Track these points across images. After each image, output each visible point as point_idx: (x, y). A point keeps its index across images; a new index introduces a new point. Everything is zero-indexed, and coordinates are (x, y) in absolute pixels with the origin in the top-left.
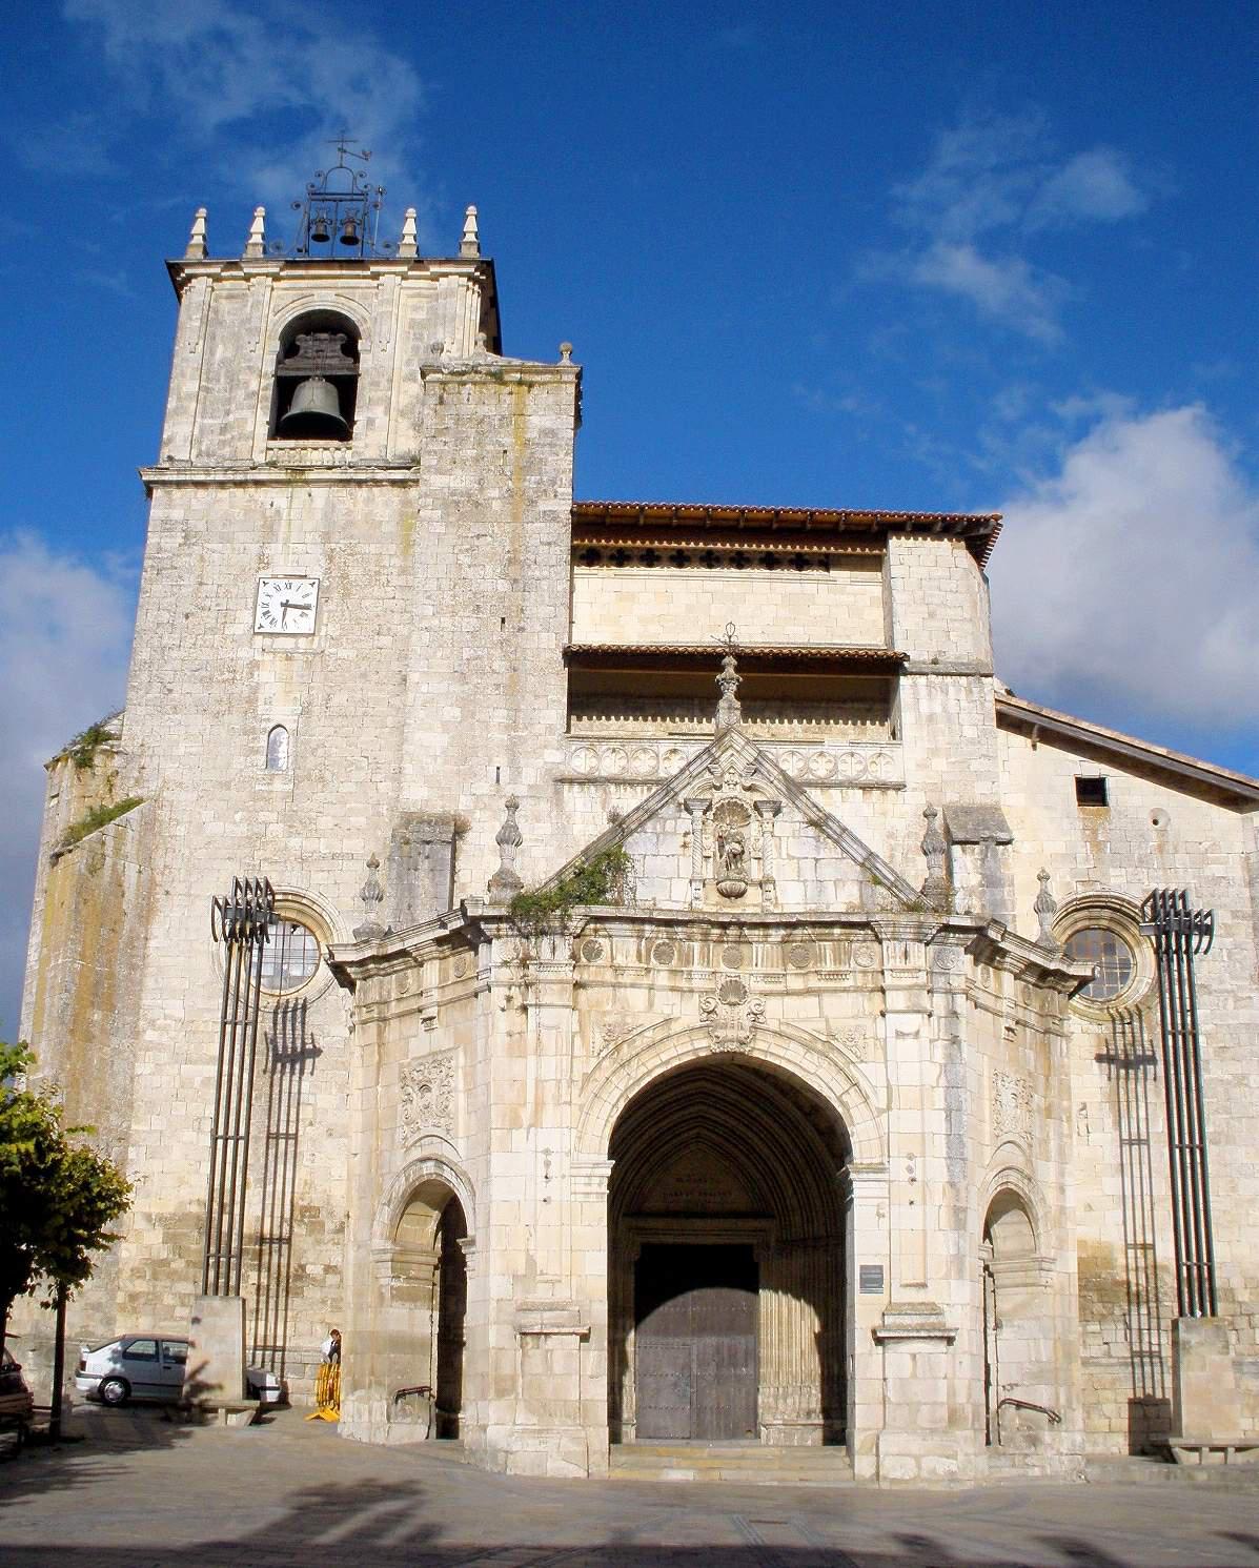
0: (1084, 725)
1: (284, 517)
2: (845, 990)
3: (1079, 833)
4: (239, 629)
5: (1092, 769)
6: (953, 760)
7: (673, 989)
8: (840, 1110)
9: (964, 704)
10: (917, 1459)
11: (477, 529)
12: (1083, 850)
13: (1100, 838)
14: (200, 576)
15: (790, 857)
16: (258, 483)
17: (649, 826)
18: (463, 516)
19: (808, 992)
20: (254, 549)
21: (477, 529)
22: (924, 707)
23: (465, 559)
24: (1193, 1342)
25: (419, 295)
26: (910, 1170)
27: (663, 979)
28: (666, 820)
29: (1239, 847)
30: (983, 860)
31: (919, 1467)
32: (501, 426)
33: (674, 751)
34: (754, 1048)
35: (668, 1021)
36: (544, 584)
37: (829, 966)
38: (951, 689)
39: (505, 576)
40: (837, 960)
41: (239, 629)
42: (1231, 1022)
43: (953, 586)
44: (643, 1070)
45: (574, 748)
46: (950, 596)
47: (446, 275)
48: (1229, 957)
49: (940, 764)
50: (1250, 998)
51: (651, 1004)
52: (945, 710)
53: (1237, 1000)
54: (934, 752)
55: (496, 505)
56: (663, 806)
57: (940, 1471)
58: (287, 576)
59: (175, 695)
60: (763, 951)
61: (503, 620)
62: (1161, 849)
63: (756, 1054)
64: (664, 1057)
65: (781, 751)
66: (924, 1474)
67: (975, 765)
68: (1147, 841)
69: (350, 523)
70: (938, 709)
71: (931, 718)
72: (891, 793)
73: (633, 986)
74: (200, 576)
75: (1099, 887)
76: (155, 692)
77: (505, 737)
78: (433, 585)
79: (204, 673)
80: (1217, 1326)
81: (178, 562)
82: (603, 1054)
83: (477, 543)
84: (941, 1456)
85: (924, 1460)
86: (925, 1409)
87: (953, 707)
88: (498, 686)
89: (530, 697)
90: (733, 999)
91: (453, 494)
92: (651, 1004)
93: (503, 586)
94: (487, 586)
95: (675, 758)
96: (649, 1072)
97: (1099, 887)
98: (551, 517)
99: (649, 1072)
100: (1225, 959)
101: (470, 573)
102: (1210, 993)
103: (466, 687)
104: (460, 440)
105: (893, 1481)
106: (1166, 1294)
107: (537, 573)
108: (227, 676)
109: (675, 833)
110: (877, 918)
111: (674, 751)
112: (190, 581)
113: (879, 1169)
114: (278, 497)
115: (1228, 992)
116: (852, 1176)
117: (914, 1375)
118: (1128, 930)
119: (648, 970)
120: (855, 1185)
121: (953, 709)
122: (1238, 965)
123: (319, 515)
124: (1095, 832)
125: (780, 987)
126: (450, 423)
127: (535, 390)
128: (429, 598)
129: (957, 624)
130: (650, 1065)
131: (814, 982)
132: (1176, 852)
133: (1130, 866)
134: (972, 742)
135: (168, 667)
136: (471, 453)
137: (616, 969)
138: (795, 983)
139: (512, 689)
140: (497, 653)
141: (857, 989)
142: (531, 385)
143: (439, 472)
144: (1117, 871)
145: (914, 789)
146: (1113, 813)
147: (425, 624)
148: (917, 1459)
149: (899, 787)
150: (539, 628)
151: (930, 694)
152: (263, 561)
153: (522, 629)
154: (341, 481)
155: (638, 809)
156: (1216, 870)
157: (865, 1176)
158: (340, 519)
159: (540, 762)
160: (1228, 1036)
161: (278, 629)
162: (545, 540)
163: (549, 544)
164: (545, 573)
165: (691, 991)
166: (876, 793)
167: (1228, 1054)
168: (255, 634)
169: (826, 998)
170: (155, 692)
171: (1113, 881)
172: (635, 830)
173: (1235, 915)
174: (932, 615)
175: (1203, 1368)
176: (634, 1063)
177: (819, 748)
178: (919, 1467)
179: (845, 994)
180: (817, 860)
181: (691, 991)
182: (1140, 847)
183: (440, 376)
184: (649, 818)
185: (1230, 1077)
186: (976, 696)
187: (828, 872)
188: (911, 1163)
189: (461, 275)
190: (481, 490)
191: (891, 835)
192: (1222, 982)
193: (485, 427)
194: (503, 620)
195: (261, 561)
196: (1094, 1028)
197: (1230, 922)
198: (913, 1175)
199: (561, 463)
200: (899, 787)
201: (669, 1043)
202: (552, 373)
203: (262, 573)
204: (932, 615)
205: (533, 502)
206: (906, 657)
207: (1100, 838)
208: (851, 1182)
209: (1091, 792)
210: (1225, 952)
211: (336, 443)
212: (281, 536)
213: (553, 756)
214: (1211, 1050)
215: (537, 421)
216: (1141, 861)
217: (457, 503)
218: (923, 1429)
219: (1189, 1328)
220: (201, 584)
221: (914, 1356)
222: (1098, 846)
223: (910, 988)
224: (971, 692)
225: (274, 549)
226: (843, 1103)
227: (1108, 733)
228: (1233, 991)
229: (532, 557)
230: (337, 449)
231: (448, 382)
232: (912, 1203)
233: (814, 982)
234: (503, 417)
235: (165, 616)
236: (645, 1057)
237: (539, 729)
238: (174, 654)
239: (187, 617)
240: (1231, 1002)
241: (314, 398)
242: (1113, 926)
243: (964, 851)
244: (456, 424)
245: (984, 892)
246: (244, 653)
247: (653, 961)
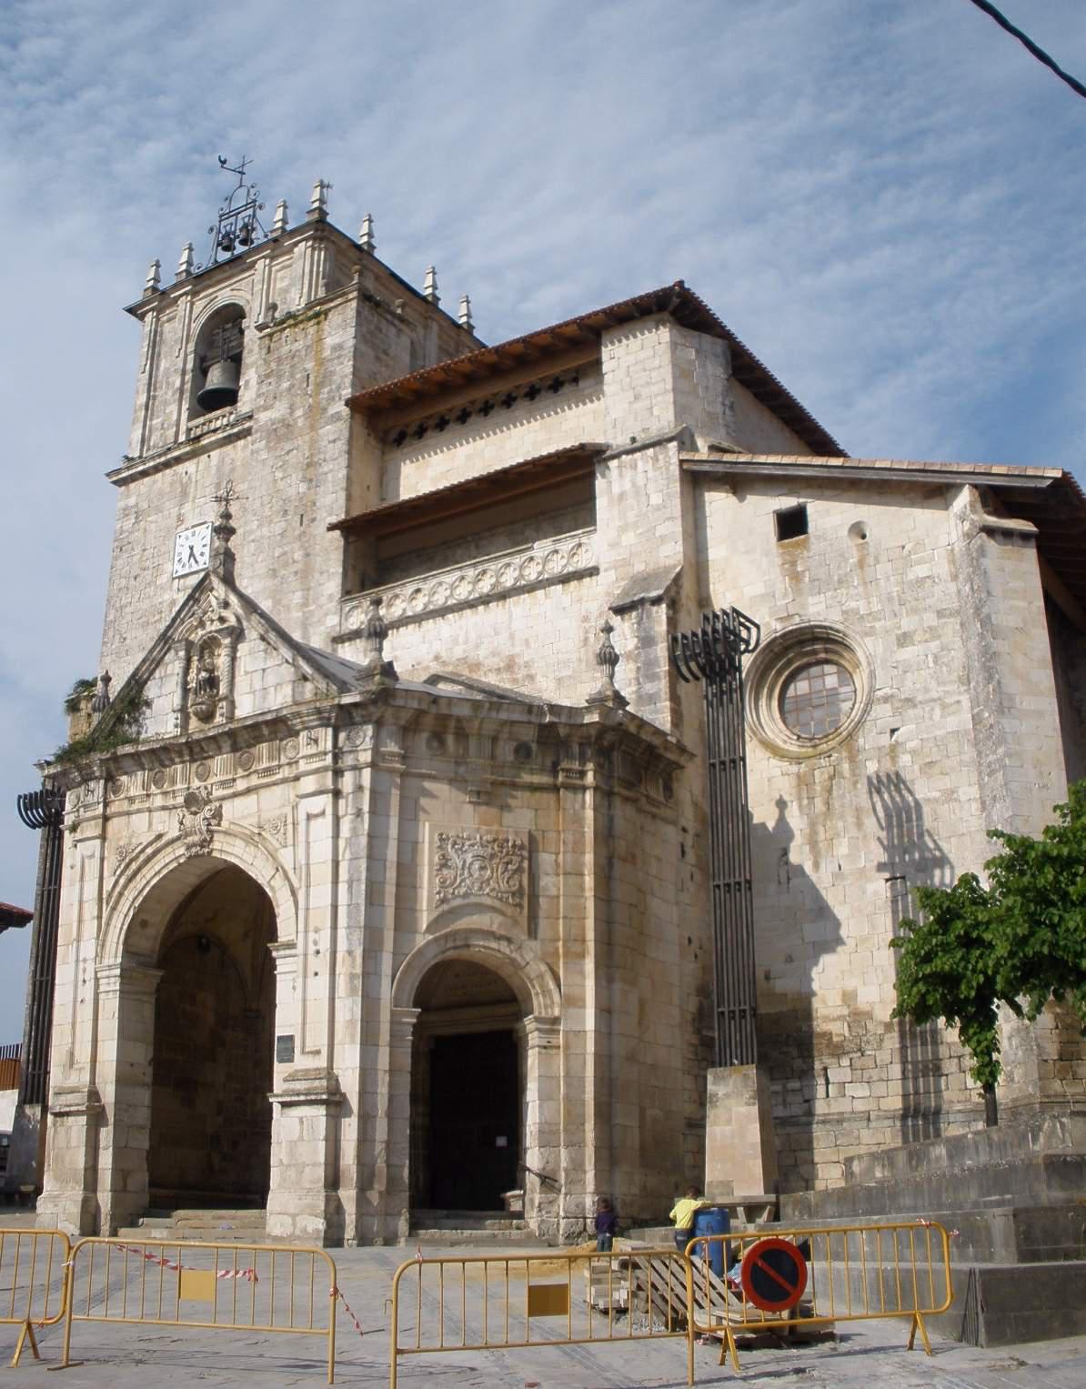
0: (762, 459)
1: (194, 480)
2: (275, 784)
3: (778, 570)
4: (164, 579)
5: (788, 502)
6: (639, 532)
7: (164, 808)
8: (270, 894)
9: (650, 474)
10: (294, 1216)
11: (288, 446)
12: (782, 584)
13: (799, 569)
14: (144, 544)
15: (246, 673)
16: (178, 460)
17: (157, 674)
18: (279, 440)
19: (248, 791)
20: (175, 512)
21: (288, 446)
22: (616, 490)
23: (279, 475)
24: (720, 1094)
25: (283, 268)
26: (315, 943)
27: (158, 801)
28: (167, 664)
29: (943, 541)
30: (639, 623)
31: (294, 1224)
32: (306, 355)
33: (418, 591)
34: (212, 850)
35: (159, 837)
36: (330, 475)
37: (265, 764)
38: (640, 464)
39: (304, 479)
40: (271, 758)
41: (164, 579)
42: (938, 733)
43: (657, 362)
44: (144, 882)
45: (347, 609)
46: (654, 374)
47: (296, 244)
48: (935, 662)
49: (629, 538)
50: (958, 702)
51: (150, 824)
52: (634, 485)
53: (944, 707)
54: (623, 529)
55: (300, 423)
56: (165, 654)
57: (310, 1229)
58: (193, 527)
59: (128, 641)
60: (220, 764)
61: (302, 516)
62: (861, 564)
63: (215, 854)
64: (157, 868)
65: (499, 566)
66: (298, 1232)
67: (660, 531)
68: (846, 560)
69: (233, 470)
70: (628, 486)
71: (622, 496)
72: (586, 580)
73: (139, 811)
74: (144, 544)
75: (797, 619)
76: (116, 643)
77: (300, 614)
78: (258, 503)
79: (144, 619)
80: (745, 1075)
81: (132, 538)
82: (118, 873)
83: (287, 458)
84: (311, 1215)
85: (298, 1218)
86: (307, 1170)
87: (640, 480)
88: (296, 573)
89: (317, 575)
90: (193, 809)
91: (273, 424)
92: (150, 824)
93: (303, 488)
94: (292, 492)
95: (420, 596)
96: (148, 882)
97: (797, 619)
98: (337, 417)
99: (148, 882)
100: (931, 665)
101: (281, 485)
102: (915, 706)
103: (276, 581)
104: (280, 377)
105: (276, 1239)
106: (868, 1042)
107: (325, 469)
108: (157, 617)
109: (172, 674)
110: (285, 712)
111: (418, 591)
112: (138, 550)
113: (291, 945)
114: (190, 466)
115: (934, 700)
116: (274, 954)
117: (301, 1138)
118: (842, 656)
119: (148, 796)
120: (278, 962)
121: (641, 482)
122: (944, 669)
123: (213, 471)
124: (793, 564)
125: (230, 791)
126: (273, 366)
127: (330, 316)
128: (255, 515)
129: (659, 398)
130: (148, 877)
131: (254, 780)
132: (877, 561)
133: (829, 590)
134: (658, 508)
135: (124, 621)
136: (285, 385)
137: (131, 800)
138: (241, 785)
139: (305, 574)
140: (296, 545)
141: (284, 781)
142: (326, 313)
143: (266, 408)
144: (817, 599)
145: (606, 570)
146: (812, 539)
147: (252, 537)
148: (294, 1216)
149: (593, 571)
150: (325, 515)
151: (621, 475)
152: (180, 519)
153: (314, 520)
154: (225, 438)
155: (144, 661)
156: (921, 571)
157: (282, 953)
158: (227, 469)
159: (323, 628)
160: (934, 749)
161: (187, 571)
162: (331, 438)
163: (334, 441)
164: (331, 467)
165: (175, 808)
166: (574, 584)
167: (936, 770)
168: (174, 579)
169: (264, 793)
170: (116, 643)
171: (812, 610)
172: (148, 679)
173: (940, 614)
174: (637, 398)
175: (729, 1122)
176: (138, 877)
177: (529, 554)
178: (294, 1224)
179: (275, 788)
180: (264, 670)
181: (175, 807)
182: (839, 567)
183: (268, 330)
184: (157, 666)
185: (937, 794)
186: (661, 463)
187: (271, 679)
188: (316, 936)
189: (306, 239)
190: (292, 413)
191: (586, 619)
192: (927, 690)
193: (296, 359)
194: (302, 516)
195: (179, 520)
196: (794, 768)
197: (935, 623)
198: (318, 947)
199: (346, 368)
200: (593, 571)
201: (159, 857)
202: (340, 296)
203: (179, 529)
204: (637, 398)
205: (325, 410)
206: (608, 447)
207: (799, 569)
208: (274, 960)
209: (792, 524)
210: (930, 658)
211: (228, 409)
212: (191, 495)
213: (332, 620)
214: (916, 767)
215: (330, 341)
216: (840, 581)
217: (275, 430)
218: (303, 1189)
219: (717, 1080)
220: (144, 550)
221: (301, 1122)
222: (796, 577)
223: (316, 771)
224: (657, 460)
225: (188, 506)
226: (272, 888)
227: (786, 460)
228: (939, 699)
229: (322, 456)
230: (231, 413)
231: (274, 333)
232: (316, 974)
233: (254, 780)
234: (308, 347)
235: (124, 582)
236: (144, 871)
237: (323, 600)
238: (128, 610)
239: (135, 578)
240: (938, 712)
241: (215, 378)
242: (830, 656)
243: (622, 619)
244: (278, 365)
245: (639, 654)
246: (167, 597)
247: (153, 787)
